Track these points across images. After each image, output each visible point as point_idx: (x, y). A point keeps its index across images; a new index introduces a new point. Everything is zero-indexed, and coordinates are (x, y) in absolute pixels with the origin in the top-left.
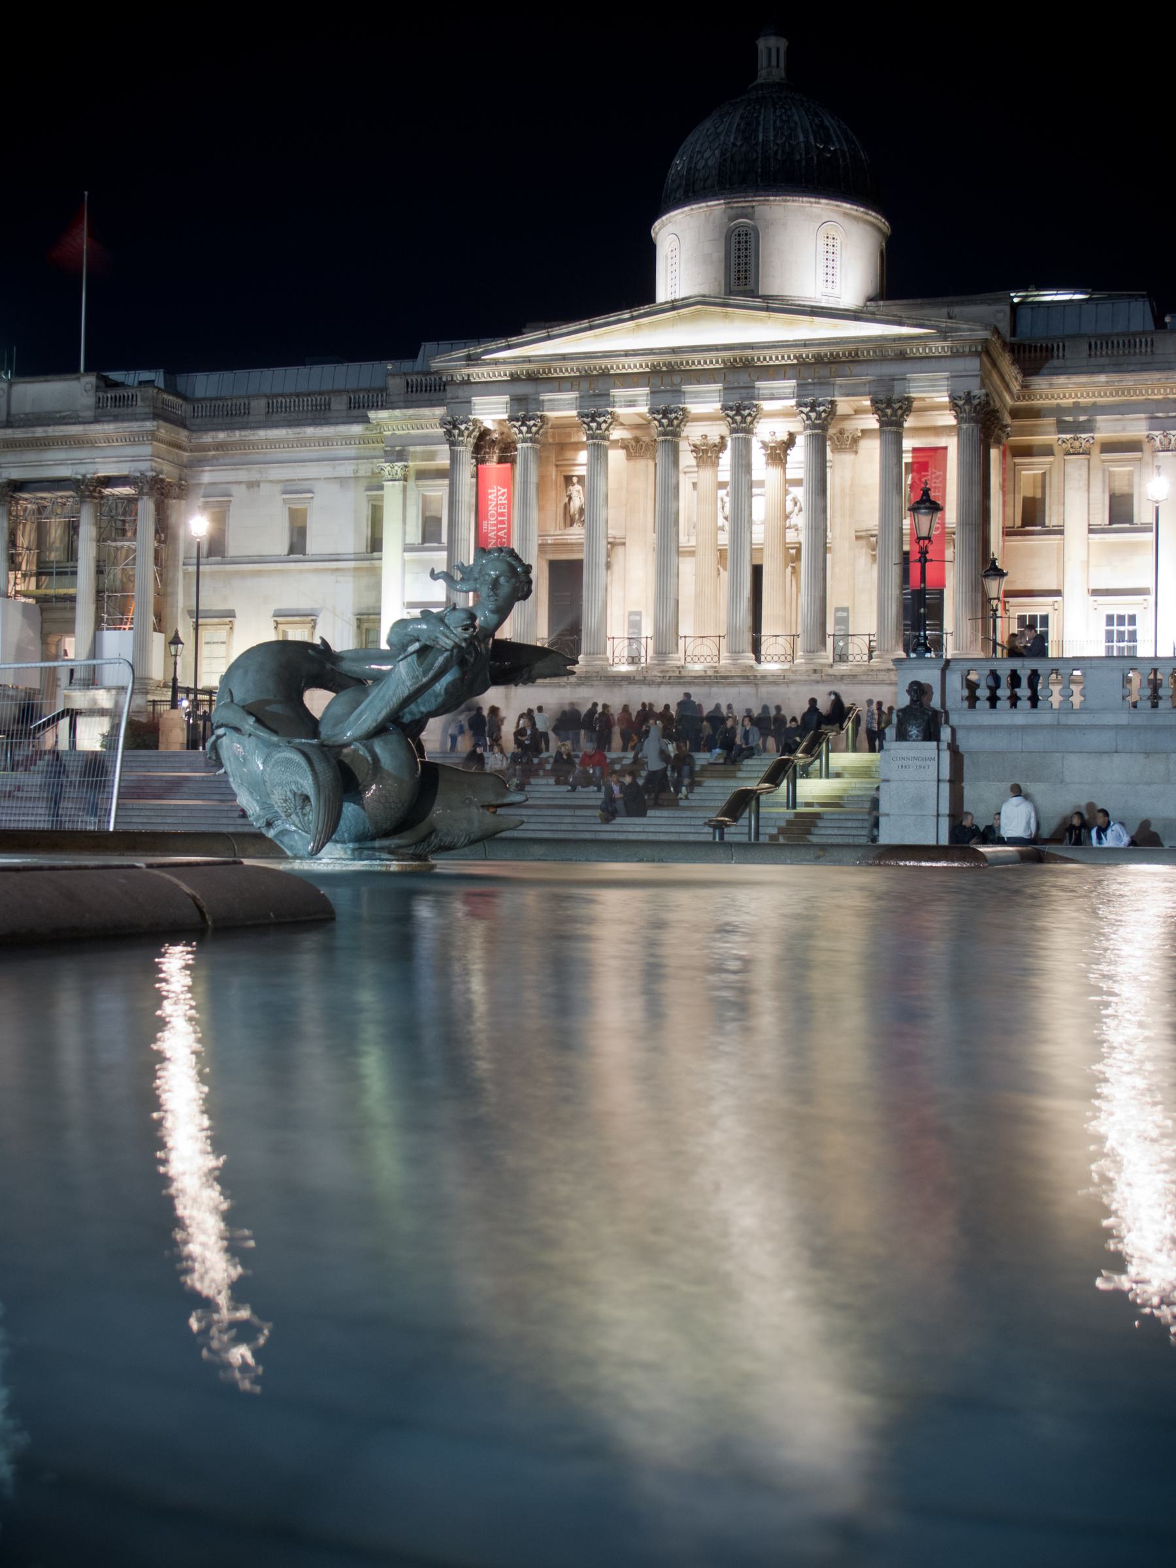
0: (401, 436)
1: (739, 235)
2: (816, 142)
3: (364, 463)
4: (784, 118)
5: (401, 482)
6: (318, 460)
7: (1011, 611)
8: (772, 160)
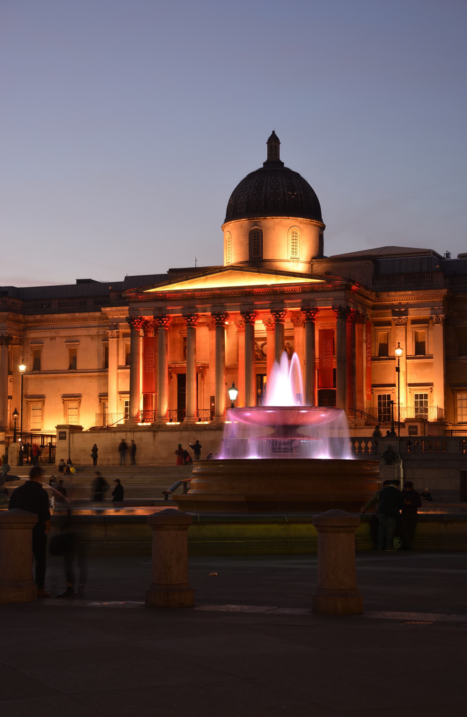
0: (116, 318)
1: (255, 233)
2: (288, 191)
3: (102, 329)
4: (275, 181)
5: (116, 339)
6: (81, 327)
7: (374, 393)
8: (268, 200)
